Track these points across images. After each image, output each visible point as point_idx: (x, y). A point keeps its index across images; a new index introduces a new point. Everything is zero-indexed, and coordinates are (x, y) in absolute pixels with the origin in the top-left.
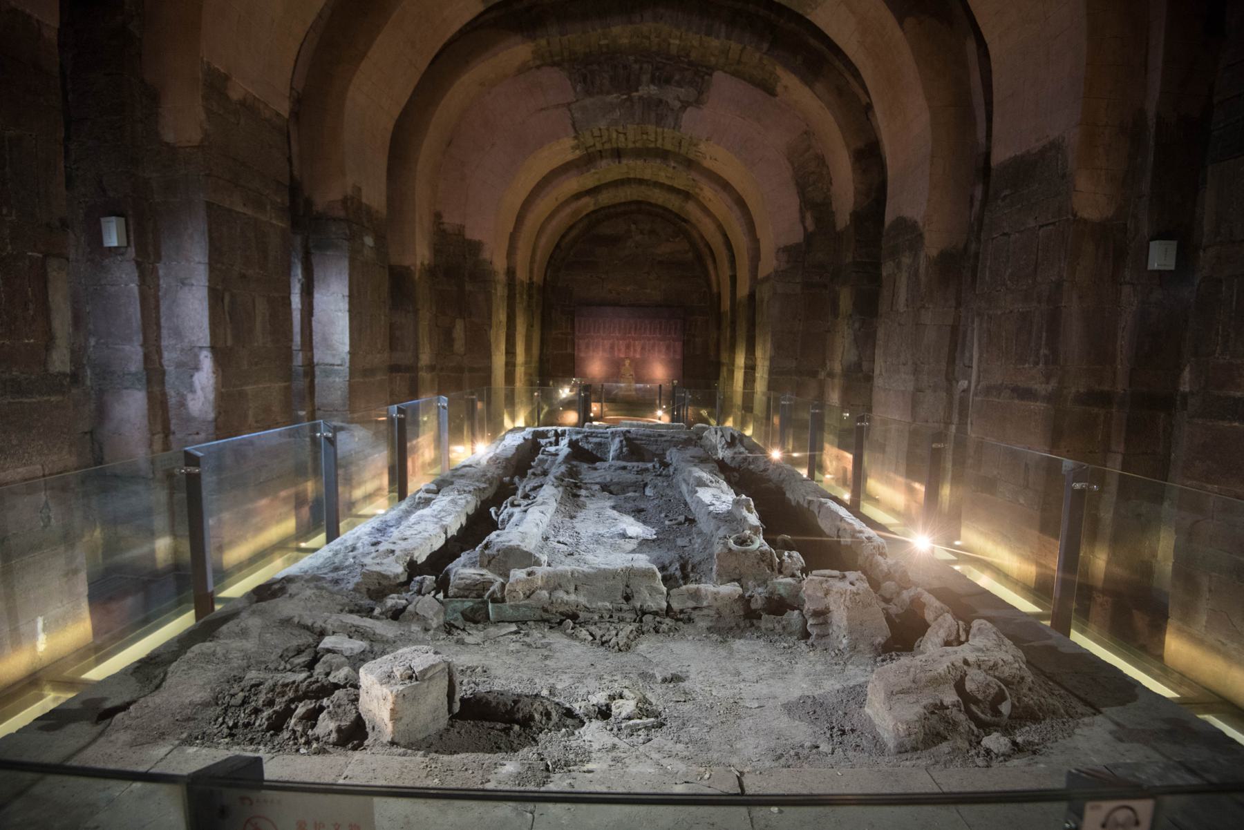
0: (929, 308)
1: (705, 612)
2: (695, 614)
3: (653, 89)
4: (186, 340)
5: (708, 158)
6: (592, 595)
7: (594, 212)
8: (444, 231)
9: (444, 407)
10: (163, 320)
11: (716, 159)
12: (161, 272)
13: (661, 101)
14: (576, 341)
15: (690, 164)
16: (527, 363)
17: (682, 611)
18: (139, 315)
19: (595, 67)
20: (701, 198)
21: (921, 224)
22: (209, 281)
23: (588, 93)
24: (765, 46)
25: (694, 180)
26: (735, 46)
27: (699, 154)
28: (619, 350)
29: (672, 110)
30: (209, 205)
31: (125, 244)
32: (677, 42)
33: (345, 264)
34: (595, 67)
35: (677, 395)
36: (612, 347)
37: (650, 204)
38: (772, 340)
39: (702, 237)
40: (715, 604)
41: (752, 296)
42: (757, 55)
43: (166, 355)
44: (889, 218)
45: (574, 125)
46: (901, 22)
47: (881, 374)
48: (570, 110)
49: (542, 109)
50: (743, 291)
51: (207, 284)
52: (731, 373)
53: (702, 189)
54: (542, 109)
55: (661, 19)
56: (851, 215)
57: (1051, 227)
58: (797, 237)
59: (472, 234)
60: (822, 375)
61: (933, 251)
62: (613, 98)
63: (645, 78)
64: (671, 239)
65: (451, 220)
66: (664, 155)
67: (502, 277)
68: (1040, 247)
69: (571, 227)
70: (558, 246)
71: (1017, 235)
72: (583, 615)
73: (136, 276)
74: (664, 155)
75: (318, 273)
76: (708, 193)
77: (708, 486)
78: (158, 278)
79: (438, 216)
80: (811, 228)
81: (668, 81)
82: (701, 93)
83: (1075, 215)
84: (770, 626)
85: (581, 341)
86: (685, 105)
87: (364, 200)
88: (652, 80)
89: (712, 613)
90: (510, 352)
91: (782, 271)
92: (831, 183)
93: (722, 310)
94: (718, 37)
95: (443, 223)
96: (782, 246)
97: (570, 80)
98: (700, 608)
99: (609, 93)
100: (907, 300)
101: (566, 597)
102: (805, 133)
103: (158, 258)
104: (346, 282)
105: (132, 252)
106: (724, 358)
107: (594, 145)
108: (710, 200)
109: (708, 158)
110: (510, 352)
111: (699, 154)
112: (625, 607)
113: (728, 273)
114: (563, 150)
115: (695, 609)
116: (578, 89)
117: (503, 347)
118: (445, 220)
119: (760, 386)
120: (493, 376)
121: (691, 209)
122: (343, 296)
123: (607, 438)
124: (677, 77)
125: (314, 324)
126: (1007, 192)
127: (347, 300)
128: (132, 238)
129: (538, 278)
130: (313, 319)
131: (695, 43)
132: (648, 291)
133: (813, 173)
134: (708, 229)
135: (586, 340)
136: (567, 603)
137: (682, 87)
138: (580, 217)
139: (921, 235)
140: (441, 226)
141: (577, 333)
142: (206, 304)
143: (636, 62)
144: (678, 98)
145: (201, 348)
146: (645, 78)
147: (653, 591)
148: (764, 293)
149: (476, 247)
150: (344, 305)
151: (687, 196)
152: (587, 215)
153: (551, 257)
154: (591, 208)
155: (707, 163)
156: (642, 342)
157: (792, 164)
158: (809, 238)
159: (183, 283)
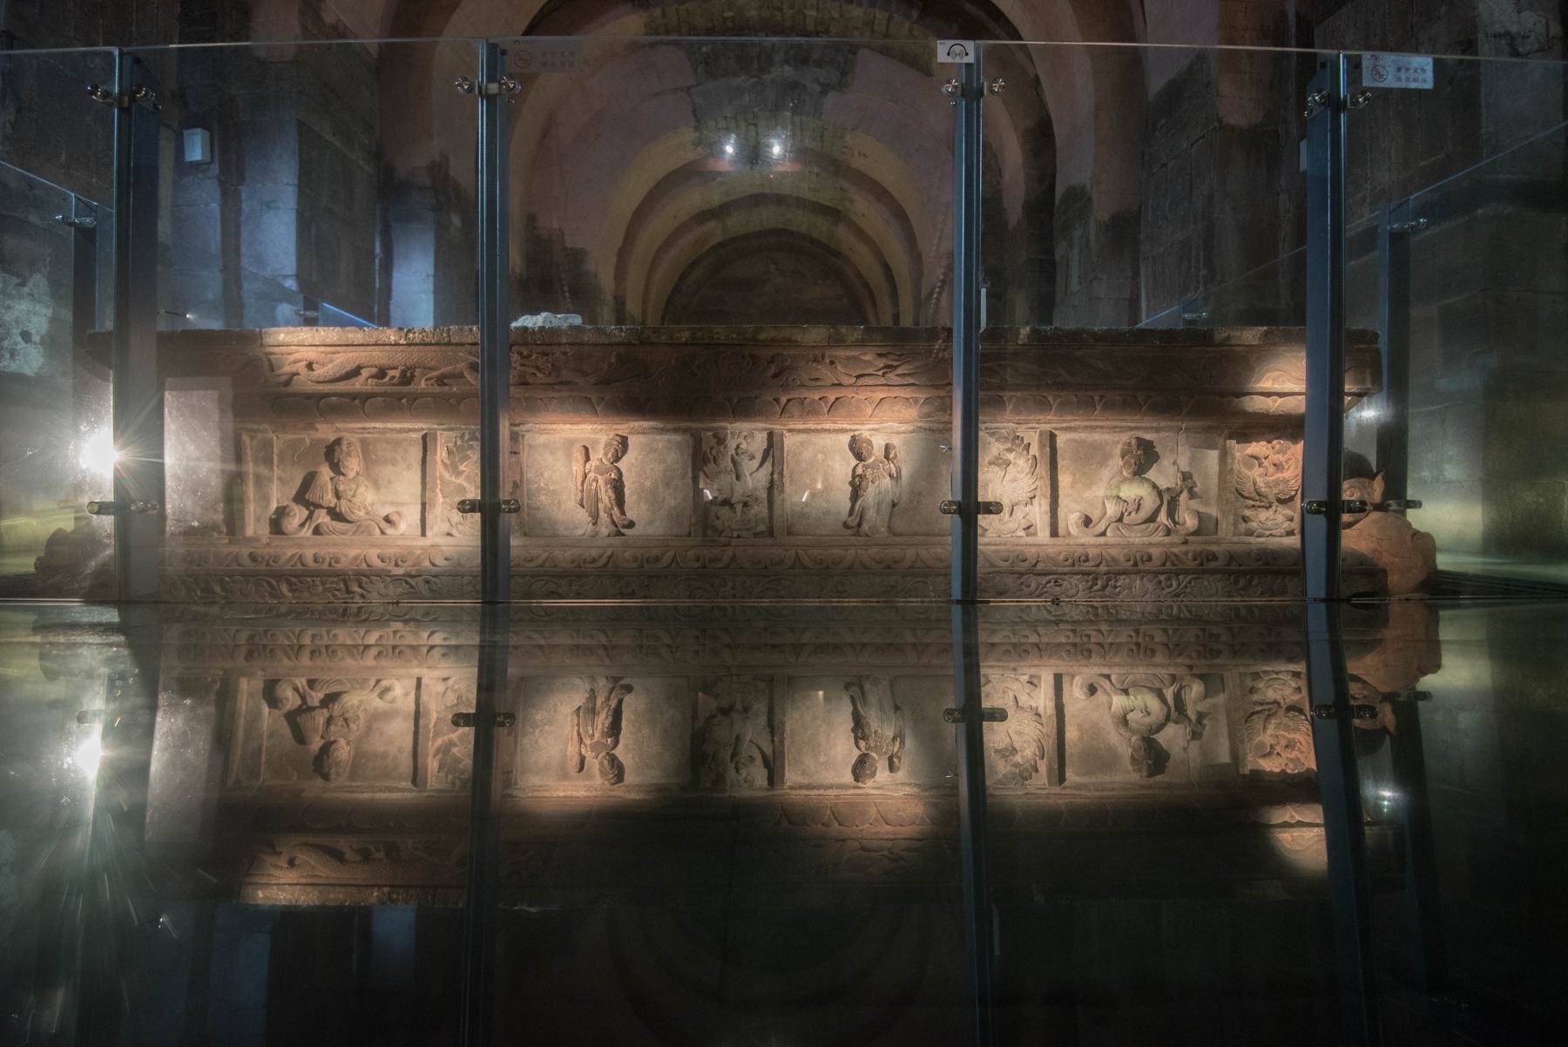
0: (1101, 279)
3: (788, 71)
4: (269, 269)
5: (856, 154)
7: (721, 245)
10: (243, 249)
11: (865, 155)
12: (244, 196)
18: (219, 238)
20: (852, 217)
21: (1089, 187)
22: (298, 204)
24: (915, 14)
25: (842, 189)
26: (880, 15)
27: (845, 150)
30: (301, 125)
31: (208, 159)
32: (814, 13)
33: (429, 240)
37: (792, 233)
39: (859, 275)
42: (907, 25)
43: (246, 286)
44: (1060, 190)
45: (694, 112)
48: (690, 95)
49: (657, 94)
51: (296, 207)
53: (852, 202)
54: (657, 94)
56: (1023, 207)
57: (1200, 141)
61: (1105, 216)
62: (741, 81)
64: (820, 282)
67: (608, 296)
68: (1193, 166)
69: (693, 265)
70: (676, 289)
71: (1174, 161)
73: (218, 195)
75: (398, 249)
76: (864, 208)
78: (241, 202)
79: (531, 219)
83: (1220, 121)
86: (824, 92)
87: (452, 173)
88: (787, 62)
92: (1001, 175)
95: (535, 228)
97: (690, 60)
100: (1079, 277)
103: (241, 179)
104: (432, 259)
105: (215, 169)
108: (863, 215)
109: (856, 154)
111: (845, 150)
116: (699, 71)
121: (842, 231)
122: (428, 275)
125: (392, 307)
126: (1163, 121)
127: (432, 279)
128: (216, 154)
130: (392, 301)
131: (835, 14)
134: (862, 256)
138: (704, 250)
139: (1090, 199)
142: (293, 229)
144: (817, 81)
145: (285, 277)
149: (578, 256)
150: (429, 286)
151: (834, 214)
152: (714, 248)
153: (669, 302)
154: (718, 239)
155: (857, 162)
159: (269, 206)
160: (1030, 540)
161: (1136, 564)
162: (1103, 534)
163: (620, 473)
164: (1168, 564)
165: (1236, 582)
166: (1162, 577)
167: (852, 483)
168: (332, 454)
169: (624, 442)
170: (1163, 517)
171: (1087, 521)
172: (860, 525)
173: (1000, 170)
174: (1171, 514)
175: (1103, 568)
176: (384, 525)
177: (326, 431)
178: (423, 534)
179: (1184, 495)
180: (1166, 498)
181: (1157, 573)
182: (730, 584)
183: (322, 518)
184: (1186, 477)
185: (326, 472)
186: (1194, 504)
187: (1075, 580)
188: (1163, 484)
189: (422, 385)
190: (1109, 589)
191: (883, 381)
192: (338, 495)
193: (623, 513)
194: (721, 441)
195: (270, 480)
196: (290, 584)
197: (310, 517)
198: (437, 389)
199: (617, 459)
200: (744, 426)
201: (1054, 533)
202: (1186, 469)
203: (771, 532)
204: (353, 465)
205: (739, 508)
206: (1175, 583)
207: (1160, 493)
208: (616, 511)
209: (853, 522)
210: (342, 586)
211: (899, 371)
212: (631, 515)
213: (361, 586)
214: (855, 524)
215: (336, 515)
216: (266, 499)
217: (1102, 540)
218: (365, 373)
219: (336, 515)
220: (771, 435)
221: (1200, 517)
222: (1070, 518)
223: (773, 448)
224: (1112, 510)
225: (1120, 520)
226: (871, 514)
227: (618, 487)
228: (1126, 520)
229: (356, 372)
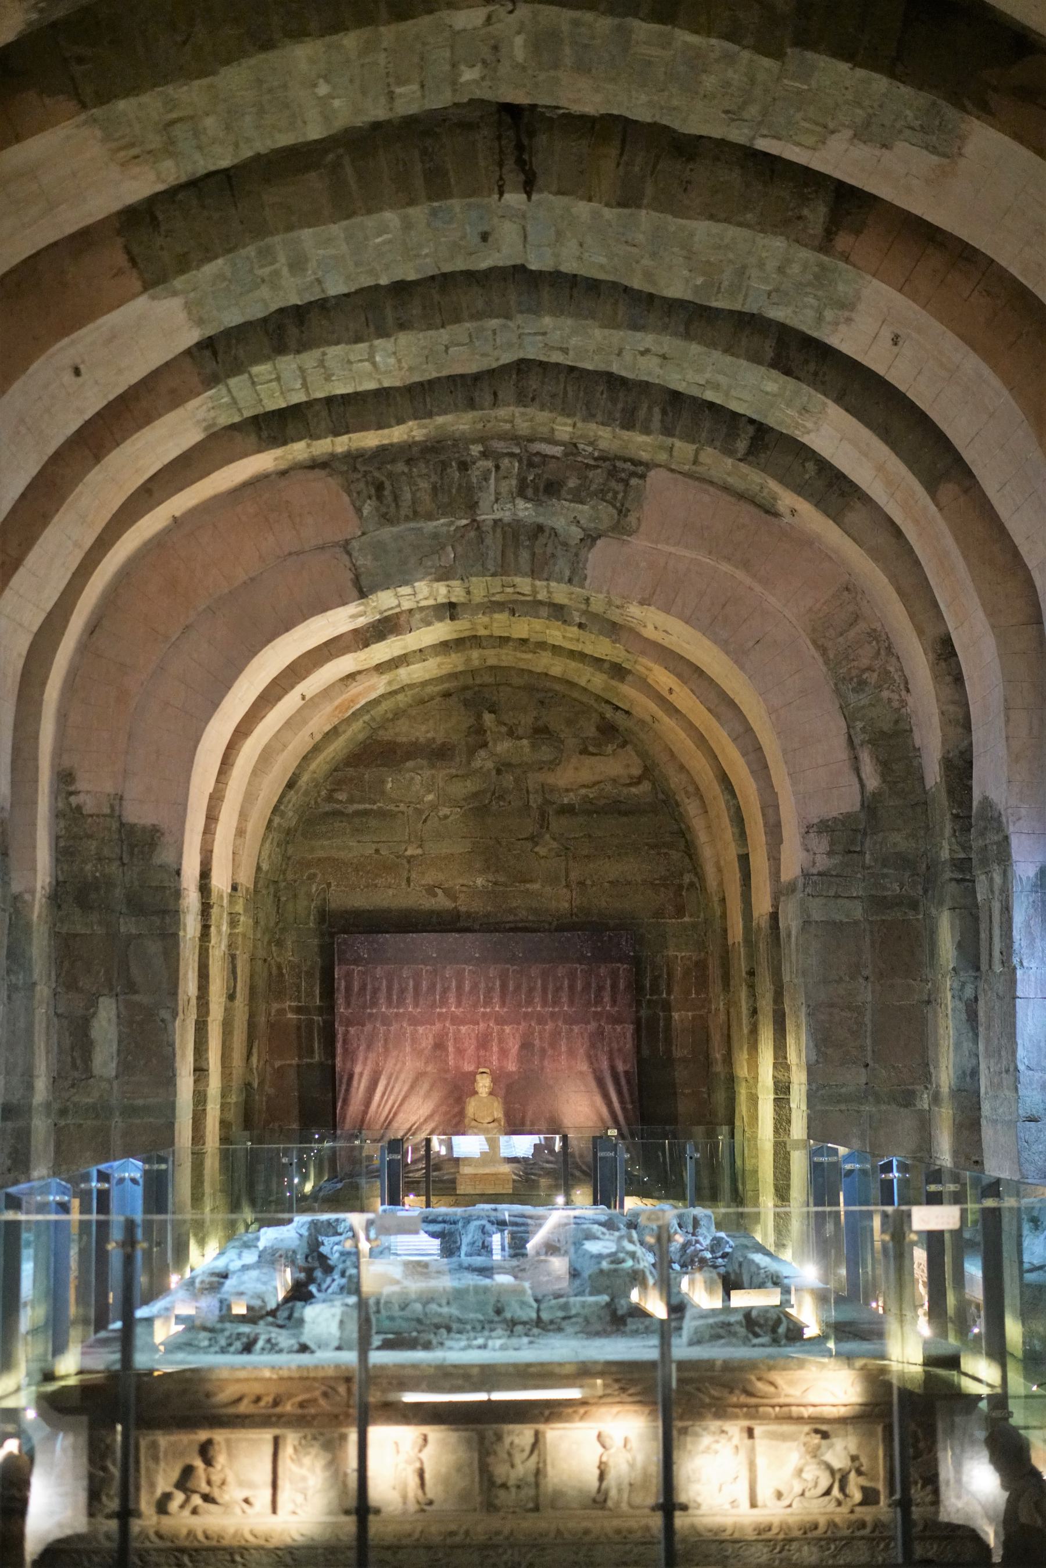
1: (574, 1320)
2: (564, 1324)
3: (524, 510)
6: (463, 1308)
9: (134, 1181)
13: (540, 528)
14: (340, 1030)
15: (614, 629)
16: (225, 1093)
17: (552, 1322)
19: (401, 467)
23: (386, 519)
28: (460, 1052)
29: (565, 544)
34: (401, 467)
35: (600, 1154)
36: (439, 1046)
38: (809, 1025)
40: (582, 1312)
41: (774, 917)
46: (931, 488)
47: (986, 1093)
48: (349, 554)
50: (762, 906)
52: (754, 1100)
55: (533, 399)
60: (924, 1102)
66: (558, 612)
72: (454, 1326)
74: (558, 612)
77: (598, 1238)
80: (873, 783)
81: (552, 489)
82: (622, 512)
84: (634, 1327)
85: (352, 1030)
86: (590, 538)
88: (521, 493)
89: (580, 1320)
90: (200, 1071)
91: (820, 874)
93: (730, 942)
94: (646, 431)
96: (816, 821)
97: (349, 493)
98: (569, 1317)
99: (430, 517)
101: (439, 1310)
102: (847, 589)
106: (742, 1071)
107: (399, 605)
110: (200, 1071)
112: (496, 1319)
113: (732, 852)
115: (564, 1318)
116: (365, 512)
117: (190, 1058)
118: (81, 785)
119: (798, 1129)
120: (177, 1125)
121: (628, 693)
123: (455, 1223)
124: (572, 483)
129: (246, 879)
132: (536, 886)
133: (870, 669)
135: (368, 1027)
136: (440, 1315)
137: (582, 503)
140: (73, 800)
141: (341, 1009)
147: (523, 1304)
148: (790, 921)
151: (618, 671)
155: (649, 632)
156: (523, 1025)
157: (823, 650)
158: (871, 806)
160: (734, 1511)
161: (805, 1533)
162: (790, 1506)
163: (422, 1463)
164: (829, 1533)
165: (878, 1544)
166: (823, 1543)
167: (599, 1467)
168: (205, 1451)
169: (425, 1440)
170: (836, 1492)
171: (779, 1495)
172: (605, 1501)
173: (906, 683)
174: (842, 1489)
175: (781, 1536)
176: (245, 1506)
177: (203, 1435)
178: (274, 1510)
179: (853, 1475)
180: (838, 1476)
181: (821, 1539)
182: (509, 1552)
183: (197, 1500)
184: (854, 1458)
185: (199, 1463)
186: (863, 1481)
187: (760, 1546)
188: (837, 1464)
189: (288, 1407)
190: (785, 1554)
191: (618, 1399)
192: (209, 1483)
193: (424, 1493)
194: (499, 1437)
195: (157, 1472)
196: (190, 1556)
197: (187, 1500)
198: (300, 1411)
199: (420, 1451)
200: (517, 1427)
201: (753, 1505)
202: (854, 1452)
203: (537, 1509)
204: (221, 1459)
205: (513, 1490)
206: (833, 1547)
207: (832, 1472)
208: (420, 1492)
209: (600, 1498)
210: (228, 1558)
211: (631, 1391)
212: (431, 1493)
213: (242, 1557)
214: (599, 1500)
215: (207, 1498)
216: (152, 1485)
217: (789, 1510)
218: (245, 1402)
219: (207, 1498)
220: (537, 1434)
221: (864, 1489)
222: (764, 1494)
223: (538, 1439)
224: (798, 1488)
225: (803, 1494)
226: (613, 1493)
227: (421, 1474)
228: (807, 1494)
229: (240, 1399)
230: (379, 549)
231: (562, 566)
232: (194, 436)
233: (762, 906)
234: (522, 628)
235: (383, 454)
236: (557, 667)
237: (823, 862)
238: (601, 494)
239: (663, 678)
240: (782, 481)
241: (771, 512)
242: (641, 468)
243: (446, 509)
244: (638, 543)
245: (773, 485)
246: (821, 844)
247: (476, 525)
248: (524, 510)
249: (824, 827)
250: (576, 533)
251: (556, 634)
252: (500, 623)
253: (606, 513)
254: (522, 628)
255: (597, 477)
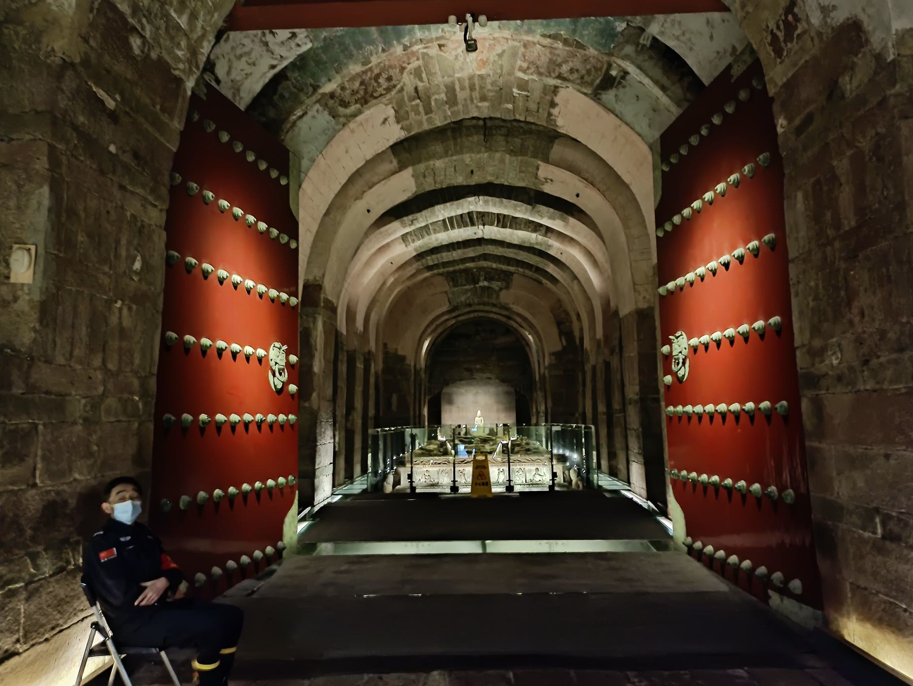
3: (486, 284)
8: (388, 352)
13: (489, 288)
19: (458, 274)
23: (455, 286)
34: (458, 274)
45: (449, 300)
58: (558, 348)
59: (400, 353)
60: (577, 415)
62: (467, 287)
63: (482, 278)
65: (392, 347)
74: (494, 305)
79: (385, 345)
80: (564, 343)
86: (501, 289)
88: (485, 280)
94: (513, 266)
99: (465, 286)
114: (445, 308)
143: (477, 271)
144: (497, 286)
146: (482, 278)
149: (403, 359)
155: (515, 310)
158: (564, 348)
230: (453, 293)
231: (494, 296)
232: (414, 271)
233: (542, 371)
234: (487, 308)
235: (454, 272)
236: (495, 316)
237: (554, 362)
238: (503, 280)
239: (519, 320)
240: (543, 277)
241: (540, 282)
242: (512, 274)
243: (468, 283)
244: (512, 291)
245: (541, 278)
246: (553, 358)
247: (475, 288)
248: (486, 284)
249: (554, 354)
250: (497, 288)
251: (494, 310)
252: (481, 307)
253: (504, 283)
254: (487, 308)
255: (502, 276)
